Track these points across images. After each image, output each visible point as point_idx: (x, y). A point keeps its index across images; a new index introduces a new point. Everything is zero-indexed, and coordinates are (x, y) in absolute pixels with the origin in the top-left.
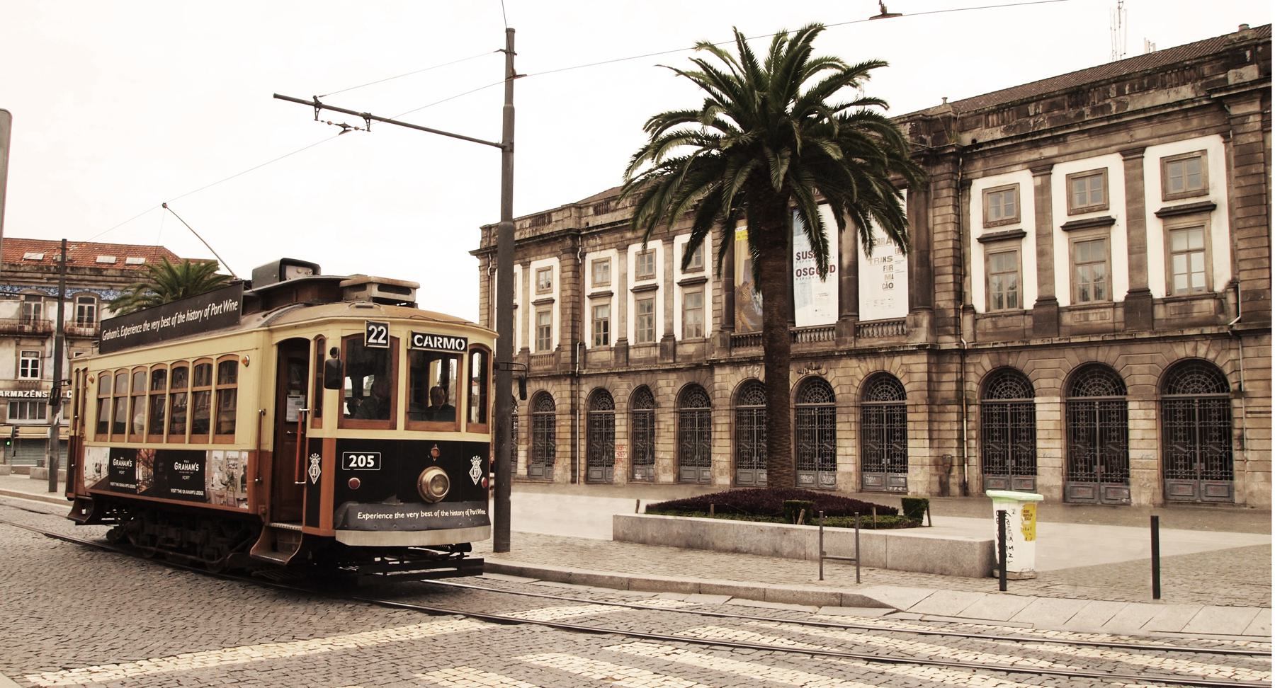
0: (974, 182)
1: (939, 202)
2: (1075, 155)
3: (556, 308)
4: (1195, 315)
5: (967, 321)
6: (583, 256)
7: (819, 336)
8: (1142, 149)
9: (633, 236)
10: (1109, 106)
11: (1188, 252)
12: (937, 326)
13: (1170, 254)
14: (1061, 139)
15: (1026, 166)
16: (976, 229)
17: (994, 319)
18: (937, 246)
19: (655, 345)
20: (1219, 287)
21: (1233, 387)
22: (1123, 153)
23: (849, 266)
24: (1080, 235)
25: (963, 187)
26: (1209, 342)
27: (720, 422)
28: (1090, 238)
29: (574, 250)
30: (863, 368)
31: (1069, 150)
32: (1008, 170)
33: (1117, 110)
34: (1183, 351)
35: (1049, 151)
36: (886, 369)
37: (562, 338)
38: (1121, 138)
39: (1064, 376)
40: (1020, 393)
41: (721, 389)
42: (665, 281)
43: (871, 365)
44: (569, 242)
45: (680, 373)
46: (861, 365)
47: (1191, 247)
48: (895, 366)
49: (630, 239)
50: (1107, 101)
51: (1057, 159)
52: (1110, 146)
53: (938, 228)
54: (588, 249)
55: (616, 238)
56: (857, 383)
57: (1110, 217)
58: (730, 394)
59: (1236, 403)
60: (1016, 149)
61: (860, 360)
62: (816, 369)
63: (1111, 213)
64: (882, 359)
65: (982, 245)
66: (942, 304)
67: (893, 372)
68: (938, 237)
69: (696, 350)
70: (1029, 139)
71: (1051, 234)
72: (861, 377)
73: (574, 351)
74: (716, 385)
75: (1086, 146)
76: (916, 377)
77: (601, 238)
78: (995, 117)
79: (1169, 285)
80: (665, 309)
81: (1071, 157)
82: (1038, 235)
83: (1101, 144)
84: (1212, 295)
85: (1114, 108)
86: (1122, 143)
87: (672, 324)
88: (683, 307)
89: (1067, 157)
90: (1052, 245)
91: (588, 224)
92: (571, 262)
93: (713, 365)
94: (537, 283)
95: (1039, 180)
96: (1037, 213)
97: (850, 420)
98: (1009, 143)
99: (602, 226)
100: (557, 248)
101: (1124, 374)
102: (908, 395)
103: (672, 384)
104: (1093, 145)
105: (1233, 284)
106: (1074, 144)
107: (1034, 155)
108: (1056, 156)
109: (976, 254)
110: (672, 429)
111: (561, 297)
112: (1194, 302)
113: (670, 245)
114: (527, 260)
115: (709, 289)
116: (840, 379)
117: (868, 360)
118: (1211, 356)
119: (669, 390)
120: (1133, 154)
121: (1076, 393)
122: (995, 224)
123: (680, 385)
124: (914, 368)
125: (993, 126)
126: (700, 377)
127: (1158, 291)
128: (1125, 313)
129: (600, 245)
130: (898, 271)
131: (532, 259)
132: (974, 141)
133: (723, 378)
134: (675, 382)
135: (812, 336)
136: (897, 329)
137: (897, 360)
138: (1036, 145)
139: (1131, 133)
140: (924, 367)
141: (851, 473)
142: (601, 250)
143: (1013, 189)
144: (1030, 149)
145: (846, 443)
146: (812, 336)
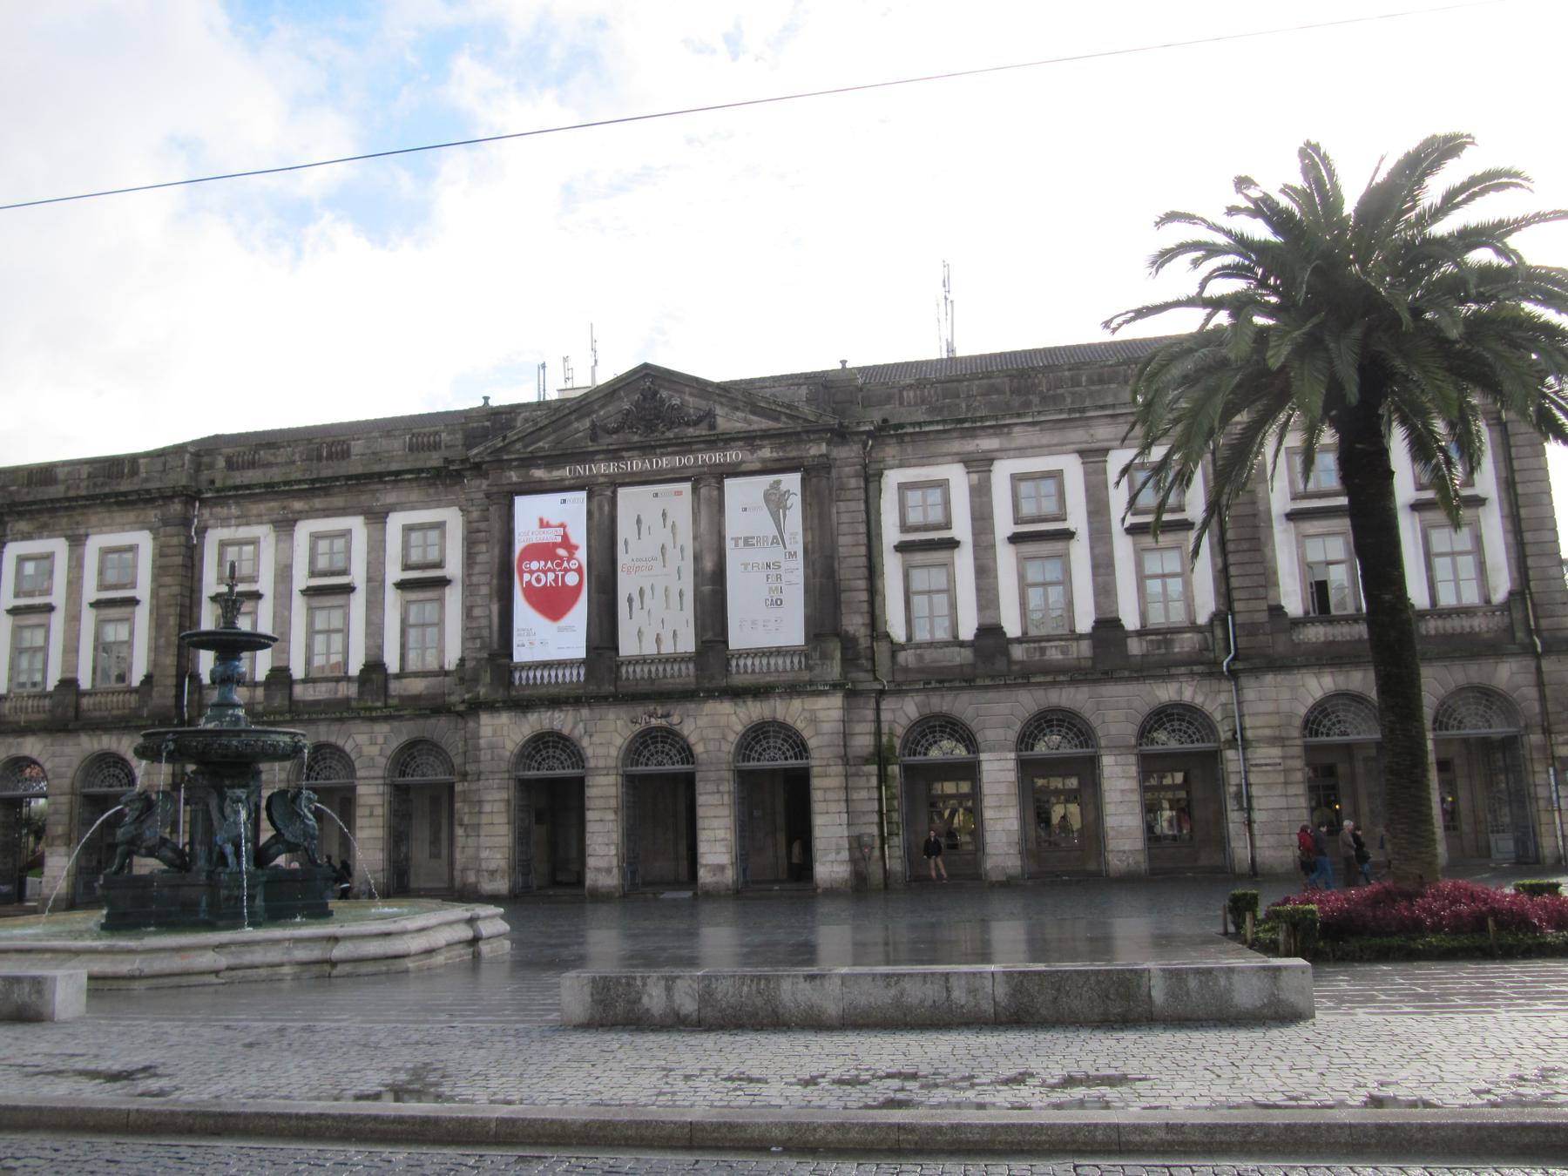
0: (886, 472)
1: (849, 495)
2: (1022, 452)
3: (142, 614)
4: (1177, 650)
5: (882, 649)
6: (202, 532)
7: (665, 670)
8: (1105, 451)
9: (306, 507)
10: (1063, 397)
11: (929, 592)
12: (851, 656)
13: (1142, 578)
14: (1006, 430)
15: (957, 458)
16: (891, 534)
17: (919, 651)
18: (842, 551)
19: (349, 679)
20: (1202, 619)
21: (1224, 734)
22: (1082, 453)
23: (714, 573)
24: (1030, 548)
25: (871, 479)
26: (1195, 683)
27: (489, 798)
28: (1044, 553)
29: (186, 522)
30: (741, 715)
31: (1013, 446)
32: (931, 460)
33: (1073, 402)
34: (1165, 693)
35: (987, 443)
36: (780, 716)
37: (155, 663)
38: (1078, 436)
39: (1018, 727)
41: (492, 747)
42: (369, 580)
43: (754, 711)
44: (176, 507)
45: (396, 724)
46: (738, 710)
47: (1167, 571)
48: (792, 711)
49: (300, 512)
50: (1060, 391)
51: (998, 454)
52: (1064, 445)
53: (844, 528)
54: (211, 522)
55: (272, 509)
56: (733, 738)
57: (1186, 520)
58: (508, 754)
59: (1230, 754)
61: (736, 704)
62: (662, 717)
63: (1069, 524)
64: (772, 702)
65: (899, 555)
66: (851, 630)
67: (789, 721)
68: (843, 540)
69: (427, 688)
70: (967, 425)
71: (992, 547)
72: (740, 728)
73: (180, 686)
74: (482, 742)
75: (1035, 442)
76: (826, 727)
77: (237, 503)
78: (912, 394)
79: (1143, 615)
80: (368, 623)
81: (1017, 452)
82: (976, 546)
83: (1055, 441)
84: (1194, 627)
85: (1069, 400)
86: (1080, 443)
87: (381, 648)
89: (1012, 453)
90: (995, 560)
91: (212, 482)
92: (182, 539)
93: (476, 707)
94: (101, 572)
95: (975, 477)
96: (974, 519)
97: (721, 788)
98: (940, 427)
99: (248, 487)
100: (153, 515)
101: (1095, 721)
102: (814, 754)
103: (380, 740)
104: (1044, 441)
105: (1219, 617)
106: (1020, 436)
107: (970, 446)
108: (997, 450)
109: (892, 566)
110: (379, 811)
111: (155, 594)
112: (1175, 637)
113: (380, 526)
114: (82, 531)
115: (453, 598)
116: (705, 732)
117: (750, 703)
118: (1199, 700)
119: (375, 750)
120: (979, 465)
121: (747, 758)
122: (917, 529)
123: (395, 743)
124: (822, 715)
125: (909, 405)
126: (439, 728)
127: (1131, 621)
128: (1095, 647)
129: (238, 517)
130: (789, 583)
131: (90, 531)
132: (885, 421)
134: (385, 737)
135: (653, 669)
136: (792, 662)
137: (797, 703)
138: (972, 433)
139: (1092, 432)
140: (836, 714)
141: (722, 868)
142: (238, 526)
143: (943, 485)
144: (963, 437)
145: (716, 823)
146: (653, 669)
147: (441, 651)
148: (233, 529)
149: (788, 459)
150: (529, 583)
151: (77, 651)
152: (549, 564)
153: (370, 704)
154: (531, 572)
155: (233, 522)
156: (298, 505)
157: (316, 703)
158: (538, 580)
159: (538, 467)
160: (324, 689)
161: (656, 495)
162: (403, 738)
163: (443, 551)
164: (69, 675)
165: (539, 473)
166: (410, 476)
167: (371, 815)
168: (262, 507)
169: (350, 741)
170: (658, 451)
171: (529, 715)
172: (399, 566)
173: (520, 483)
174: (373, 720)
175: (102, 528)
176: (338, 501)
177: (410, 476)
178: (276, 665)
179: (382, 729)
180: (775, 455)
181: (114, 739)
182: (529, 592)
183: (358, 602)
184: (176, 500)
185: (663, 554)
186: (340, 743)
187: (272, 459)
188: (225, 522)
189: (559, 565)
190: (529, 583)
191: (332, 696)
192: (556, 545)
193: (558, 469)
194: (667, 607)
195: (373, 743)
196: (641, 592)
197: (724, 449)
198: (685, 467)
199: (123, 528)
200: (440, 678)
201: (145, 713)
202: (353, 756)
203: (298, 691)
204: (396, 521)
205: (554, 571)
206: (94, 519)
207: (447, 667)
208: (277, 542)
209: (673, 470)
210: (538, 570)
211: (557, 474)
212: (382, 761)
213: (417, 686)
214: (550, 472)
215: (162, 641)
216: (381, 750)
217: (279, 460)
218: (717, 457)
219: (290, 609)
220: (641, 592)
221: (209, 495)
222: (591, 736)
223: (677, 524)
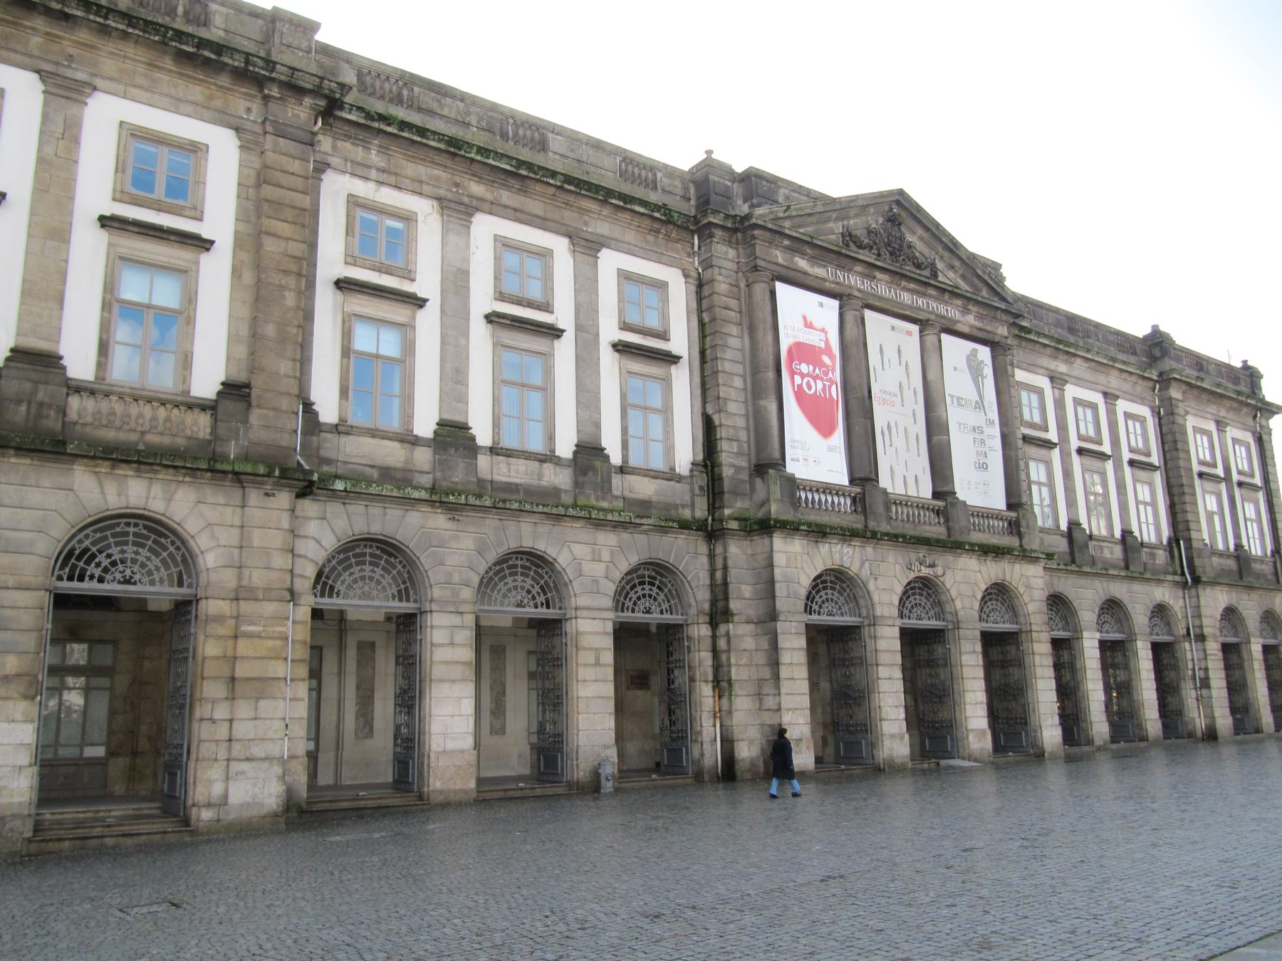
40: (664, 607)
41: (788, 581)
44: (300, 112)
45: (625, 536)
54: (334, 161)
55: (437, 179)
60: (1042, 351)
62: (930, 566)
77: (383, 150)
80: (580, 388)
87: (597, 425)
88: (623, 396)
103: (606, 556)
119: (598, 569)
133: (789, 560)
134: (612, 554)
142: (381, 183)
147: (669, 449)
148: (371, 186)
149: (986, 331)
150: (800, 386)
151: (60, 300)
152: (817, 371)
153: (594, 502)
154: (803, 376)
155: (373, 174)
156: (477, 189)
157: (511, 488)
158: (809, 387)
159: (803, 254)
160: (522, 468)
161: (893, 328)
162: (634, 559)
163: (665, 316)
164: (35, 343)
165: (802, 263)
166: (642, 210)
167: (597, 664)
168: (422, 171)
169: (565, 553)
170: (904, 283)
171: (820, 545)
172: (614, 323)
173: (784, 266)
174: (599, 524)
175: (126, 87)
176: (534, 206)
177: (642, 210)
178: (447, 416)
179: (608, 539)
180: (977, 324)
181: (157, 490)
182: (799, 394)
183: (565, 351)
184: (308, 101)
185: (901, 392)
186: (551, 551)
187: (435, 106)
188: (359, 170)
189: (826, 374)
190: (800, 386)
191: (535, 482)
192: (821, 351)
193: (820, 266)
194: (908, 450)
195: (596, 559)
196: (889, 427)
197: (946, 303)
198: (919, 309)
199: (176, 105)
200: (672, 483)
201: (232, 450)
202: (570, 573)
203: (483, 461)
204: (610, 262)
205: (822, 379)
206: (109, 65)
207: (677, 470)
208: (445, 231)
209: (910, 307)
210: (808, 375)
211: (819, 271)
212: (611, 588)
213: (644, 488)
214: (812, 266)
215: (270, 330)
216: (608, 568)
217: (446, 112)
218: (942, 309)
219: (466, 334)
220: (889, 427)
221: (352, 117)
222: (876, 579)
223: (909, 364)
